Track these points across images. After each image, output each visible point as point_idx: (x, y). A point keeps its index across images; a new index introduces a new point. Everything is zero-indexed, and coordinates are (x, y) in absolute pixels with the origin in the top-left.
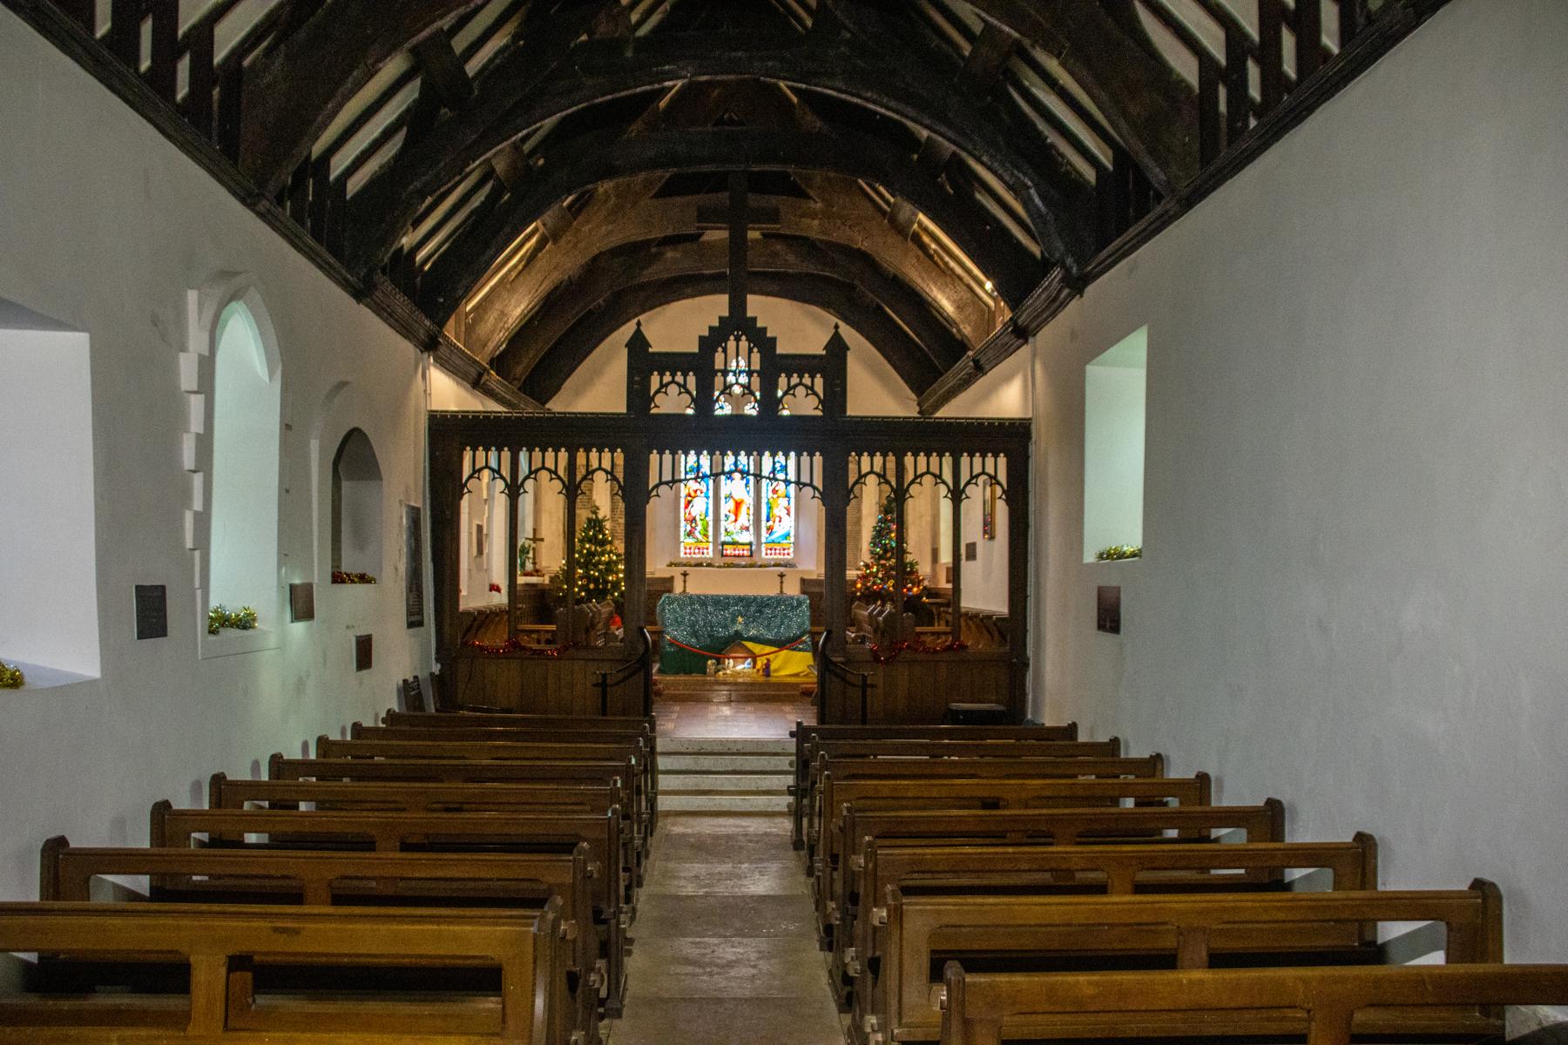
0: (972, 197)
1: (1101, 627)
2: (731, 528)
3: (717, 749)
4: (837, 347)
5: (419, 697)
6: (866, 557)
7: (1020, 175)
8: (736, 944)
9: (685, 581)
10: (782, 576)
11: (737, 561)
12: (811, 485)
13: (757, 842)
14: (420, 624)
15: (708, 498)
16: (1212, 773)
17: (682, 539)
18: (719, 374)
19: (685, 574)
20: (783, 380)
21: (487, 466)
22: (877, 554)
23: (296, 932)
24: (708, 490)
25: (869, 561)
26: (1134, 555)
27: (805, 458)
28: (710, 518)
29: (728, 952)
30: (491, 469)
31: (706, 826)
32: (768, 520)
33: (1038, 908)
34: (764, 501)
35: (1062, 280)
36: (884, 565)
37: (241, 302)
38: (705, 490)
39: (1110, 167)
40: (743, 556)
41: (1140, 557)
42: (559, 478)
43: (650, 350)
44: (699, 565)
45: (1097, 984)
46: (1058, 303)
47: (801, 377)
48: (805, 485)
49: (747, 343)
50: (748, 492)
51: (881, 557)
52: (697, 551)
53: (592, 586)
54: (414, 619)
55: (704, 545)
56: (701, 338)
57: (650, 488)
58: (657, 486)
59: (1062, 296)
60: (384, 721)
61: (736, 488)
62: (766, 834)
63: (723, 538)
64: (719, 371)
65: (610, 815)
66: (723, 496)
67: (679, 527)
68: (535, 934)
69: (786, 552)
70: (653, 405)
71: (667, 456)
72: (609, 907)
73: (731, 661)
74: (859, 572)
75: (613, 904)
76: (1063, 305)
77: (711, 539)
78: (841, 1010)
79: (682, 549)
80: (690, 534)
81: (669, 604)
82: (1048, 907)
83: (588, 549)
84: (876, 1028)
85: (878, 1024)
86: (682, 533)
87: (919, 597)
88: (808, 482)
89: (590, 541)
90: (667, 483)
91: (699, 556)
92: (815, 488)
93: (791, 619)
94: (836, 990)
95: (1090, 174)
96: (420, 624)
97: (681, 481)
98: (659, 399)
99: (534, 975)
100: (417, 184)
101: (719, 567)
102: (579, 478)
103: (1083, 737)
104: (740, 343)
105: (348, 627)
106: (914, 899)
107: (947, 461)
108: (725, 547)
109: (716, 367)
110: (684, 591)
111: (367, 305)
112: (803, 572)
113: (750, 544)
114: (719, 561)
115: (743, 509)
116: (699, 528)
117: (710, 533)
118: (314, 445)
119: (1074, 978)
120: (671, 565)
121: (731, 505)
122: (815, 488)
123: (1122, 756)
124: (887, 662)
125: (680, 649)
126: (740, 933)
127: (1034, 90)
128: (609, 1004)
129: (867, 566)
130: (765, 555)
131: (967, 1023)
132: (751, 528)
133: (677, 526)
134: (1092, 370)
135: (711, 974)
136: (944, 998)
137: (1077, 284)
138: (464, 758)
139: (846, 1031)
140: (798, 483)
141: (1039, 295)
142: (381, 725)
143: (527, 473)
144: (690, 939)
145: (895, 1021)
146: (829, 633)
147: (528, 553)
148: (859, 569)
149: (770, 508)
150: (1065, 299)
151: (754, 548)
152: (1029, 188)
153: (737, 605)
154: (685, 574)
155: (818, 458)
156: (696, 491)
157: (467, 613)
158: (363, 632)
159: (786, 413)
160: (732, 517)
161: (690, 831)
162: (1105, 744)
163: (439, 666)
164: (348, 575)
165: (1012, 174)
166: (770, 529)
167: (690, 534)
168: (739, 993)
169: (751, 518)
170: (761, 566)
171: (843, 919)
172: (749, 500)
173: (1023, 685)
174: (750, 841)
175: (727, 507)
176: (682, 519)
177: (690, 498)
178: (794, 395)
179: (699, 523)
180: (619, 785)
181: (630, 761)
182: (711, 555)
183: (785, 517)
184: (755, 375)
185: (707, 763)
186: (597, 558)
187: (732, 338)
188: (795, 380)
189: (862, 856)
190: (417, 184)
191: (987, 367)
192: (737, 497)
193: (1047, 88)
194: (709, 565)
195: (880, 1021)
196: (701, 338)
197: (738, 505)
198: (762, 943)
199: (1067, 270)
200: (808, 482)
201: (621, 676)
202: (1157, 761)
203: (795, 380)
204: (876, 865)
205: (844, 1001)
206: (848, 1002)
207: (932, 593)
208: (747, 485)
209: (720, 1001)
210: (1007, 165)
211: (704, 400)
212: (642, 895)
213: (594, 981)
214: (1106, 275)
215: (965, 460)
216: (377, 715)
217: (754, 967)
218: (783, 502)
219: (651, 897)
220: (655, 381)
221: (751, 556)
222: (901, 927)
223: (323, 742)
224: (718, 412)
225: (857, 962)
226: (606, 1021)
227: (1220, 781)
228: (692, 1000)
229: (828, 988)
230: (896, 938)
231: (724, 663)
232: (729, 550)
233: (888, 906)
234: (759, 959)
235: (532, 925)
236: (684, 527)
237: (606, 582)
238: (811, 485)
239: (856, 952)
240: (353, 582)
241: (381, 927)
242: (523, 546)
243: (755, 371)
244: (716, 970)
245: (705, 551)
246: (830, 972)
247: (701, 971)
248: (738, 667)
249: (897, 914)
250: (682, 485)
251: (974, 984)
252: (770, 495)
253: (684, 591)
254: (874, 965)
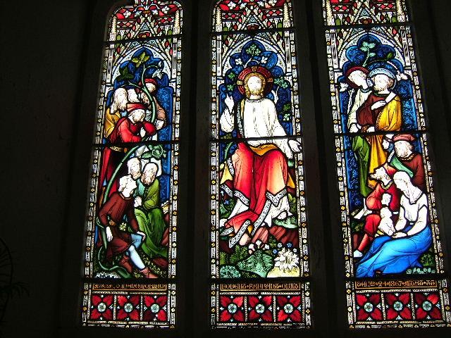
15: (166, 143)
24: (169, 123)
38: (160, 124)
50: (286, 125)
69: (427, 306)
77: (173, 270)
91: (135, 324)
149: (359, 166)
166: (368, 234)
177: (116, 149)
179: (140, 216)
183: (414, 192)
208: (282, 109)
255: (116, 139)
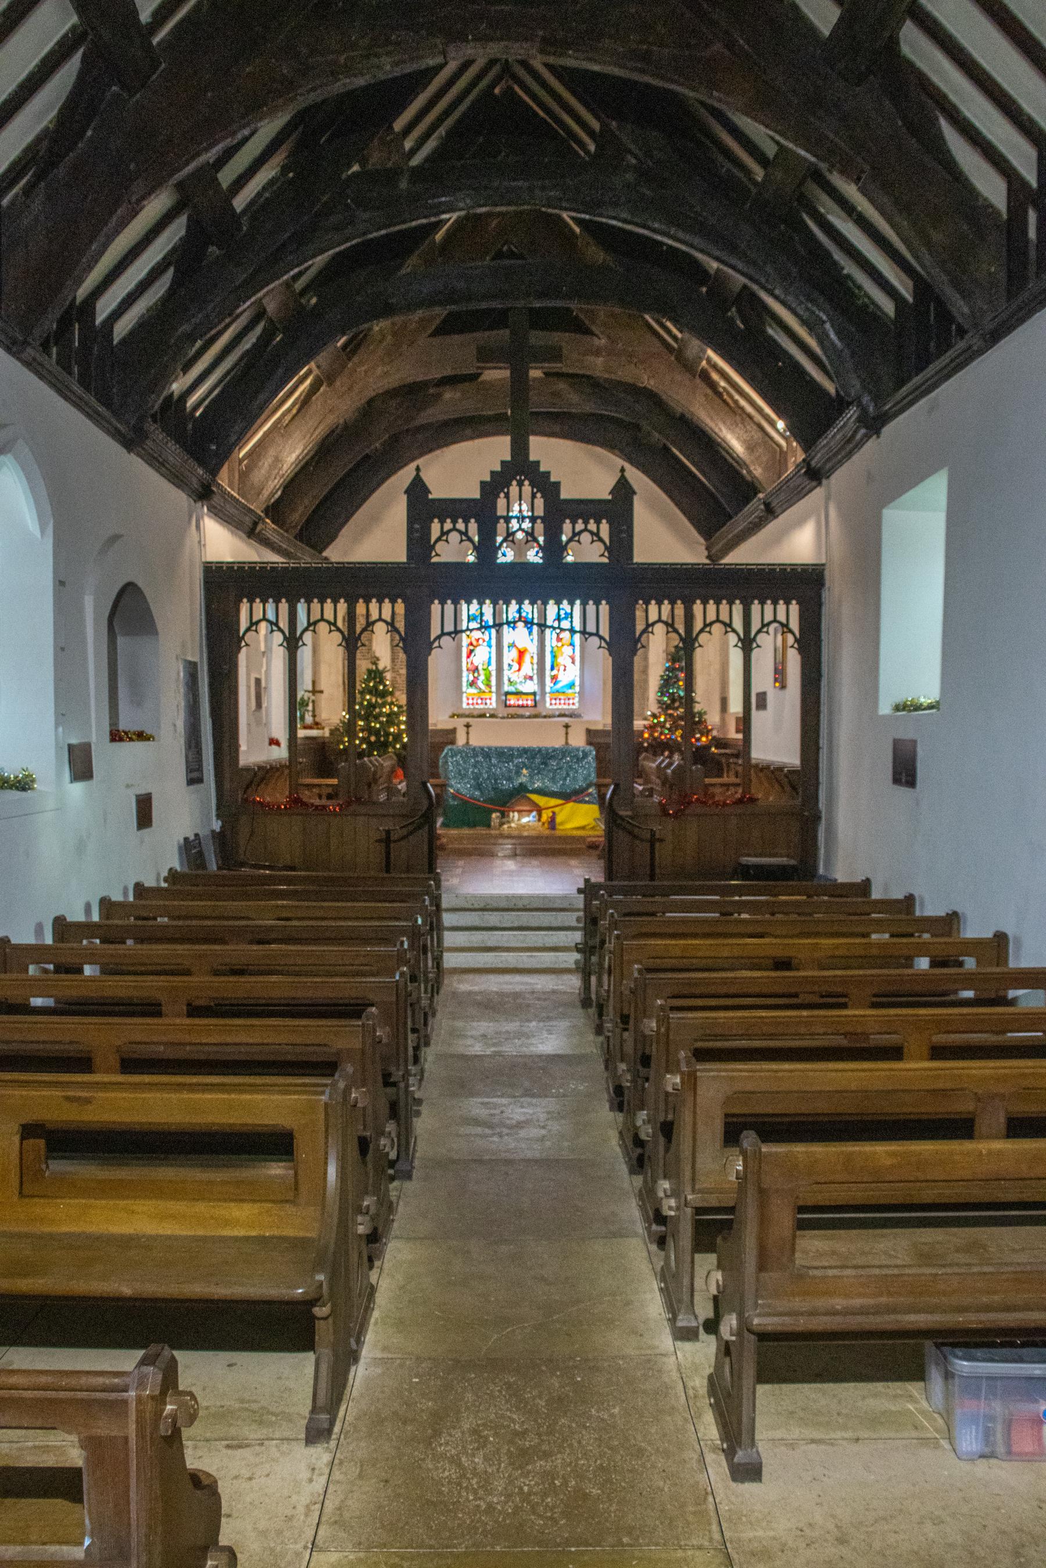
0: (764, 332)
1: (896, 780)
2: (514, 677)
3: (503, 905)
4: (623, 491)
5: (201, 854)
6: (653, 707)
7: (814, 308)
8: (525, 1104)
9: (468, 733)
10: (567, 726)
11: (520, 711)
12: (597, 634)
13: (545, 1000)
14: (200, 780)
15: (490, 646)
16: (1010, 932)
17: (464, 689)
18: (502, 521)
19: (468, 726)
20: (567, 526)
21: (264, 619)
22: (665, 703)
23: (88, 1101)
25: (656, 711)
26: (930, 707)
27: (591, 607)
28: (493, 667)
29: (517, 1112)
30: (268, 621)
31: (493, 984)
32: (552, 668)
33: (834, 1074)
34: (548, 649)
35: (859, 420)
36: (671, 715)
37: (9, 455)
39: (910, 300)
40: (527, 706)
41: (938, 709)
42: (338, 630)
43: (430, 497)
44: (483, 716)
45: (894, 1154)
46: (854, 443)
47: (586, 523)
48: (591, 634)
49: (530, 488)
51: (668, 707)
52: (480, 701)
53: (373, 739)
54: (195, 775)
55: (487, 696)
56: (483, 484)
57: (432, 639)
58: (439, 637)
59: (858, 437)
60: (166, 880)
61: (519, 637)
62: (554, 992)
63: (506, 688)
64: (501, 517)
65: (397, 978)
66: (505, 644)
67: (461, 677)
68: (326, 1104)
69: (571, 701)
70: (434, 553)
71: (449, 606)
72: (398, 1070)
73: (516, 814)
74: (646, 723)
75: (402, 1067)
76: (859, 445)
77: (494, 689)
78: (632, 1172)
79: (464, 699)
80: (472, 684)
81: (452, 757)
82: (844, 1074)
83: (369, 701)
84: (669, 1193)
85: (671, 1189)
86: (464, 684)
87: (707, 747)
88: (594, 631)
89: (370, 693)
90: (449, 634)
91: (482, 706)
92: (601, 638)
93: (577, 772)
94: (627, 1153)
95: (888, 307)
96: (200, 780)
97: (464, 631)
98: (440, 547)
99: (326, 1143)
100: (186, 328)
101: (503, 718)
102: (358, 629)
103: (876, 894)
104: (523, 488)
105: (128, 786)
106: (708, 1066)
107: (738, 608)
108: (509, 697)
109: (499, 514)
110: (468, 743)
111: (138, 455)
112: (588, 722)
113: (534, 694)
114: (504, 712)
115: (527, 658)
116: (482, 678)
117: (493, 682)
118: (89, 602)
119: (872, 1149)
120: (453, 716)
121: (514, 654)
122: (601, 638)
123: (918, 913)
124: (676, 816)
125: (465, 804)
126: (528, 1093)
127: (830, 218)
128: (398, 1166)
129: (654, 716)
130: (550, 705)
131: (762, 1192)
132: (535, 677)
133: (459, 676)
134: (889, 514)
135: (501, 1136)
136: (740, 1168)
137: (874, 424)
138: (248, 918)
139: (637, 1191)
140: (584, 632)
141: (833, 437)
142: (164, 885)
143: (305, 624)
144: (480, 1100)
145: (688, 1189)
146: (617, 786)
147: (307, 705)
148: (645, 719)
149: (554, 657)
150: (862, 440)
151: (538, 698)
152: (824, 322)
153: (521, 757)
154: (468, 726)
155: (604, 608)
156: (478, 640)
157: (247, 769)
158: (142, 791)
159: (570, 559)
160: (516, 666)
161: (476, 988)
162: (897, 901)
163: (220, 823)
164: (126, 733)
165: (807, 309)
166: (554, 678)
167: (472, 684)
168: (529, 1155)
169: (535, 667)
170: (545, 717)
171: (633, 1081)
172: (533, 648)
173: (815, 838)
174: (539, 999)
175: (510, 656)
176: (464, 668)
177: (471, 648)
178: (579, 541)
179: (481, 672)
180: (406, 946)
181: (416, 921)
182: (494, 705)
184: (539, 521)
185: (493, 919)
186: (377, 710)
187: (514, 483)
188: (580, 526)
189: (655, 1021)
190: (186, 328)
191: (779, 511)
192: (520, 646)
193: (843, 214)
194: (492, 716)
195: (674, 1187)
196: (483, 484)
197: (521, 654)
198: (550, 1104)
199: (864, 410)
200: (594, 631)
201: (405, 831)
202: (953, 919)
203: (580, 526)
204: (668, 1029)
205: (635, 1162)
206: (639, 1164)
207: (720, 743)
209: (509, 1162)
210: (802, 298)
211: (486, 548)
212: (429, 1055)
213: (385, 1146)
214: (901, 417)
215: (756, 607)
216: (158, 874)
217: (544, 1127)
218: (567, 650)
219: (440, 1057)
220: (435, 528)
221: (535, 706)
222: (695, 1093)
223: (106, 904)
224: (501, 560)
225: (649, 1126)
226: (396, 1184)
227: (1018, 941)
228: (480, 1162)
229: (618, 1149)
230: (689, 1104)
231: (508, 816)
232: (512, 701)
233: (682, 1074)
234: (548, 1119)
235: (323, 1093)
236: (466, 677)
237: (387, 734)
238: (597, 634)
239: (648, 1115)
240: (131, 740)
241: (173, 1096)
242: (302, 699)
243: (538, 517)
244: (505, 1131)
245: (488, 701)
246: (620, 1133)
247: (488, 1131)
248: (524, 820)
249: (691, 1081)
250: (464, 635)
251: (770, 1154)
252: (555, 643)
253: (468, 743)
254: (667, 1130)
255: (471, 644)
